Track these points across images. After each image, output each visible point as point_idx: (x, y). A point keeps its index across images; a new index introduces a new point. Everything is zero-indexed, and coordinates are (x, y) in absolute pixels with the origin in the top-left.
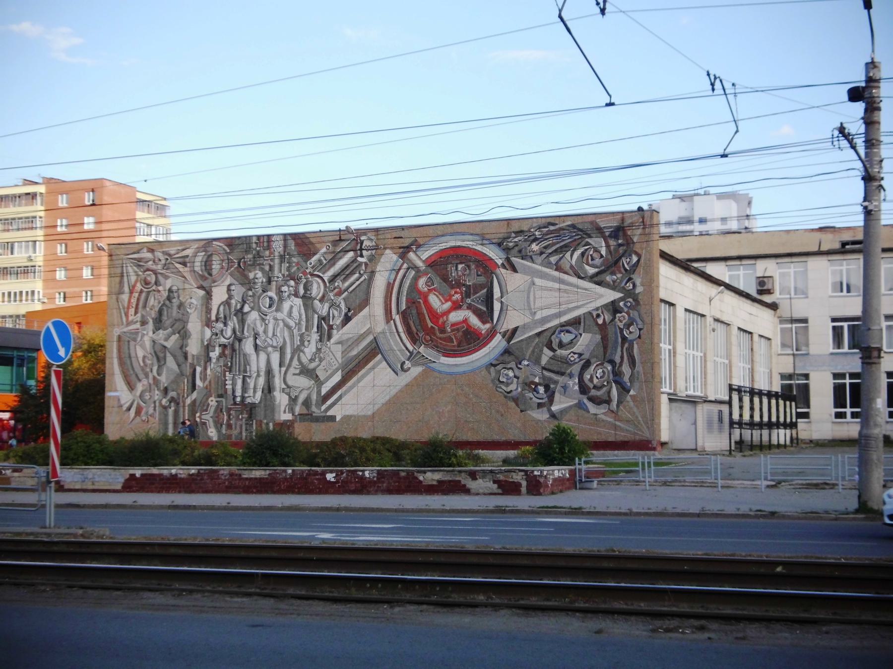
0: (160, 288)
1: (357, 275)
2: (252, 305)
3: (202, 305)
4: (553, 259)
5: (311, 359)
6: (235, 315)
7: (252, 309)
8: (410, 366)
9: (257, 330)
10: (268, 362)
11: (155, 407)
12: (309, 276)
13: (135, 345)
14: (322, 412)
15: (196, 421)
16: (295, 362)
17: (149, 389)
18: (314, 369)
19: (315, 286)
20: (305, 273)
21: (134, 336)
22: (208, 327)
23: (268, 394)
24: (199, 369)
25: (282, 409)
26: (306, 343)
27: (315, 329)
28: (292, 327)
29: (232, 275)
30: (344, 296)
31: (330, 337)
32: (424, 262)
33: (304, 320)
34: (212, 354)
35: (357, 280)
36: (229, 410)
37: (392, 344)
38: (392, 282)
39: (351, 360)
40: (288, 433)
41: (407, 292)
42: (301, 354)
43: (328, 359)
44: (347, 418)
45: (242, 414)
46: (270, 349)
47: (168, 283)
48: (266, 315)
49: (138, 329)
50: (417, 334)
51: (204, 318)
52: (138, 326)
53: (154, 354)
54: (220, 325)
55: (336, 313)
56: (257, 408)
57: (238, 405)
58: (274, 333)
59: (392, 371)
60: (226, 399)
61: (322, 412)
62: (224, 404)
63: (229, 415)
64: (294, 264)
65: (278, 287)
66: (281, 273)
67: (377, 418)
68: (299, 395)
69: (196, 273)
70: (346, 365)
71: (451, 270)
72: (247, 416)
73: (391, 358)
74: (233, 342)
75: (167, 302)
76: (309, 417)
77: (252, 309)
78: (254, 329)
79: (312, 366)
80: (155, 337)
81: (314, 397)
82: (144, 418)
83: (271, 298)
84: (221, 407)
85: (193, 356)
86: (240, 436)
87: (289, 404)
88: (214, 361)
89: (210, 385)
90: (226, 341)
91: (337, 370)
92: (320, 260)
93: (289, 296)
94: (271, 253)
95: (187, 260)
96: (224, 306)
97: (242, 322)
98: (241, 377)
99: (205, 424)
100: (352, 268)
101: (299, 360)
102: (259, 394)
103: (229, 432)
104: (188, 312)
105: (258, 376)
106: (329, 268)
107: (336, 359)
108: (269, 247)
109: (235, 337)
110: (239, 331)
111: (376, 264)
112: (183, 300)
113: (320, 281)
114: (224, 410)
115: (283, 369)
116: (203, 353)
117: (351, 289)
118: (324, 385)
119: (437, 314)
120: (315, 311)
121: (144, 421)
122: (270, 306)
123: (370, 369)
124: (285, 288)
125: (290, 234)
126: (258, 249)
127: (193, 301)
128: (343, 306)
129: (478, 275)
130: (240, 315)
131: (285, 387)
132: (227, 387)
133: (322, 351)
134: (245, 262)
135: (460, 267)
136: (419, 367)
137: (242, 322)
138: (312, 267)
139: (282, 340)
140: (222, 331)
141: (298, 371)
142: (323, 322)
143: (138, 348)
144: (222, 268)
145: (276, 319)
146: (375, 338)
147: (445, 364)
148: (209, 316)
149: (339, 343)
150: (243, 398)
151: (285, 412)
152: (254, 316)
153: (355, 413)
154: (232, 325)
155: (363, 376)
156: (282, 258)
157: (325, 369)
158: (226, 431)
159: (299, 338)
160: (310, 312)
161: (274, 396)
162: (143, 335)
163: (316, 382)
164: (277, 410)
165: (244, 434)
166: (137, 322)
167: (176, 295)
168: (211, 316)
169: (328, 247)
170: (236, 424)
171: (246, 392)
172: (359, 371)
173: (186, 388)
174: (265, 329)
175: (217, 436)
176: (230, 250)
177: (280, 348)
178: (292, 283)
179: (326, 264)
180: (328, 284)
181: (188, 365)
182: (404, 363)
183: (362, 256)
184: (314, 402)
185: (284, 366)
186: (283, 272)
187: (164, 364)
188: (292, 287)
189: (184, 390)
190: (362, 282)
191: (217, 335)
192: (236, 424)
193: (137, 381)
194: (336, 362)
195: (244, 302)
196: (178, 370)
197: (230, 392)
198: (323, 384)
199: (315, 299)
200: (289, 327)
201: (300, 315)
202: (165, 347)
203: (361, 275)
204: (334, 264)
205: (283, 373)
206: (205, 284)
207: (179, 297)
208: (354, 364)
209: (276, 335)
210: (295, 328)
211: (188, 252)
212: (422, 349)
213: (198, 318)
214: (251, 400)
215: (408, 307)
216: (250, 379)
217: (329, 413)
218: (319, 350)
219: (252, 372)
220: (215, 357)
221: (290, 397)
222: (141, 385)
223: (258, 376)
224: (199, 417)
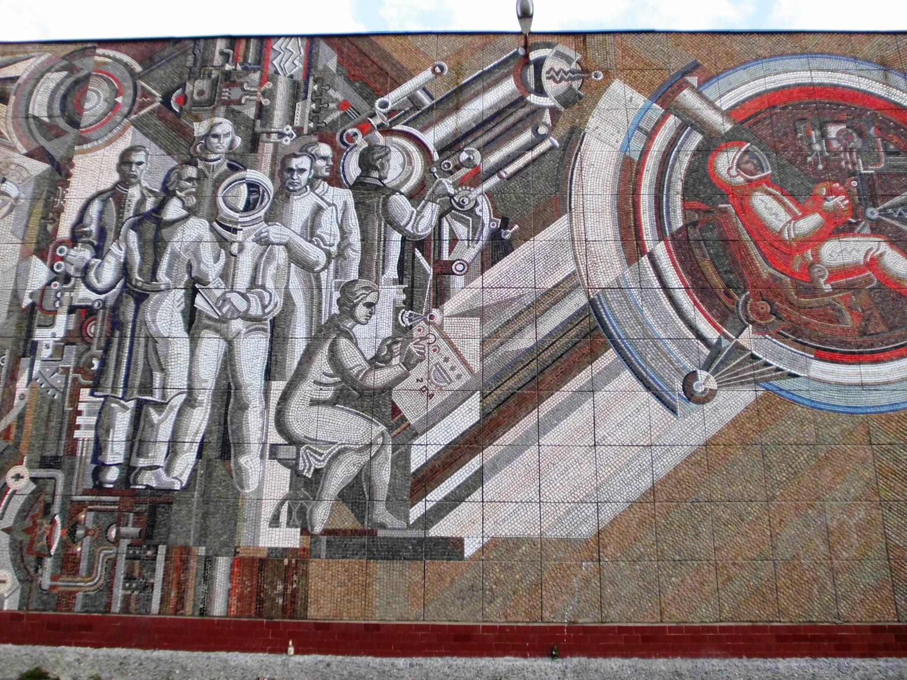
1: (526, 136)
2: (193, 201)
3: (34, 199)
5: (376, 357)
6: (134, 227)
8: (713, 384)
9: (199, 271)
10: (228, 362)
12: (377, 134)
14: (410, 527)
16: (321, 364)
18: (387, 389)
19: (395, 161)
20: (365, 128)
22: (43, 259)
23: (219, 464)
25: (267, 512)
27: (392, 272)
28: (317, 263)
29: (140, 125)
30: (487, 185)
31: (441, 295)
32: (728, 114)
33: (358, 246)
34: (42, 335)
35: (530, 147)
36: (72, 511)
37: (651, 320)
38: (637, 159)
39: (515, 362)
40: (283, 595)
41: (685, 183)
42: (343, 342)
43: (436, 358)
45: (119, 523)
46: (237, 325)
48: (235, 231)
50: (728, 295)
54: (84, 254)
55: (462, 231)
56: (175, 507)
57: (109, 492)
58: (254, 279)
59: (653, 400)
60: (70, 473)
61: (410, 527)
62: (60, 489)
64: (332, 106)
65: (279, 158)
66: (292, 124)
67: (610, 549)
68: (329, 467)
69: (31, 120)
70: (497, 377)
71: (810, 137)
72: (136, 530)
73: (653, 365)
74: (119, 300)
76: (365, 540)
77: (192, 212)
78: (190, 266)
79: (381, 377)
81: (384, 475)
83: (253, 187)
84: (48, 499)
86: (105, 600)
87: (291, 498)
88: (45, 353)
89: (20, 427)
90: (94, 296)
91: (465, 393)
92: (412, 98)
93: (311, 183)
94: (263, 80)
95: (12, 87)
96: (105, 202)
97: (156, 247)
98: (131, 404)
100: (511, 120)
101: (334, 357)
102: (186, 461)
103: (63, 583)
105: (190, 402)
106: (442, 118)
107: (465, 363)
108: (262, 60)
109: (125, 286)
110: (140, 271)
111: (584, 116)
113: (411, 147)
114: (56, 509)
115: (278, 386)
116: (12, 330)
117: (510, 169)
118: (421, 439)
119: (783, 241)
120: (392, 223)
122: (250, 206)
123: (581, 391)
125: (328, 38)
126: (228, 67)
128: (485, 211)
129: (889, 153)
130: (150, 228)
131: (280, 440)
132: (77, 434)
133: (416, 334)
134: (183, 99)
135: (833, 131)
136: (745, 388)
138: (389, 114)
139: (279, 300)
140: (87, 268)
141: (328, 394)
142: (418, 254)
144: (114, 107)
145: (264, 242)
146: (592, 302)
147: (829, 383)
148: (50, 228)
149: (480, 313)
150: (129, 470)
151: (275, 521)
153: (535, 533)
154: (122, 254)
155: (560, 414)
156: (297, 92)
157: (423, 390)
158: (54, 578)
159: (337, 295)
160: (377, 225)
161: (239, 468)
163: (390, 428)
164: (248, 513)
165: (119, 592)
168: (56, 230)
169: (438, 70)
170: (92, 557)
171: (139, 455)
172: (541, 400)
174: (227, 265)
175: (17, 595)
176: (145, 69)
177: (273, 322)
178: (325, 149)
179: (431, 108)
180: (436, 157)
182: (692, 376)
183: (540, 91)
184: (382, 493)
185: (282, 378)
186: (297, 123)
188: (324, 158)
190: (543, 154)
191: (67, 278)
192: (92, 557)
194: (461, 369)
195: (167, 193)
197: (85, 451)
198: (416, 435)
199: (394, 191)
200: (306, 266)
201: (344, 234)
203: (542, 138)
204: (457, 108)
206: (56, 148)
208: (524, 375)
209: (263, 287)
210: (326, 267)
211: (21, 70)
212: (747, 338)
213: (13, 232)
214: (158, 477)
215: (689, 224)
216: (160, 412)
217: (438, 530)
218: (402, 332)
219: (170, 393)
220: (51, 342)
221: (296, 474)
223: (190, 402)
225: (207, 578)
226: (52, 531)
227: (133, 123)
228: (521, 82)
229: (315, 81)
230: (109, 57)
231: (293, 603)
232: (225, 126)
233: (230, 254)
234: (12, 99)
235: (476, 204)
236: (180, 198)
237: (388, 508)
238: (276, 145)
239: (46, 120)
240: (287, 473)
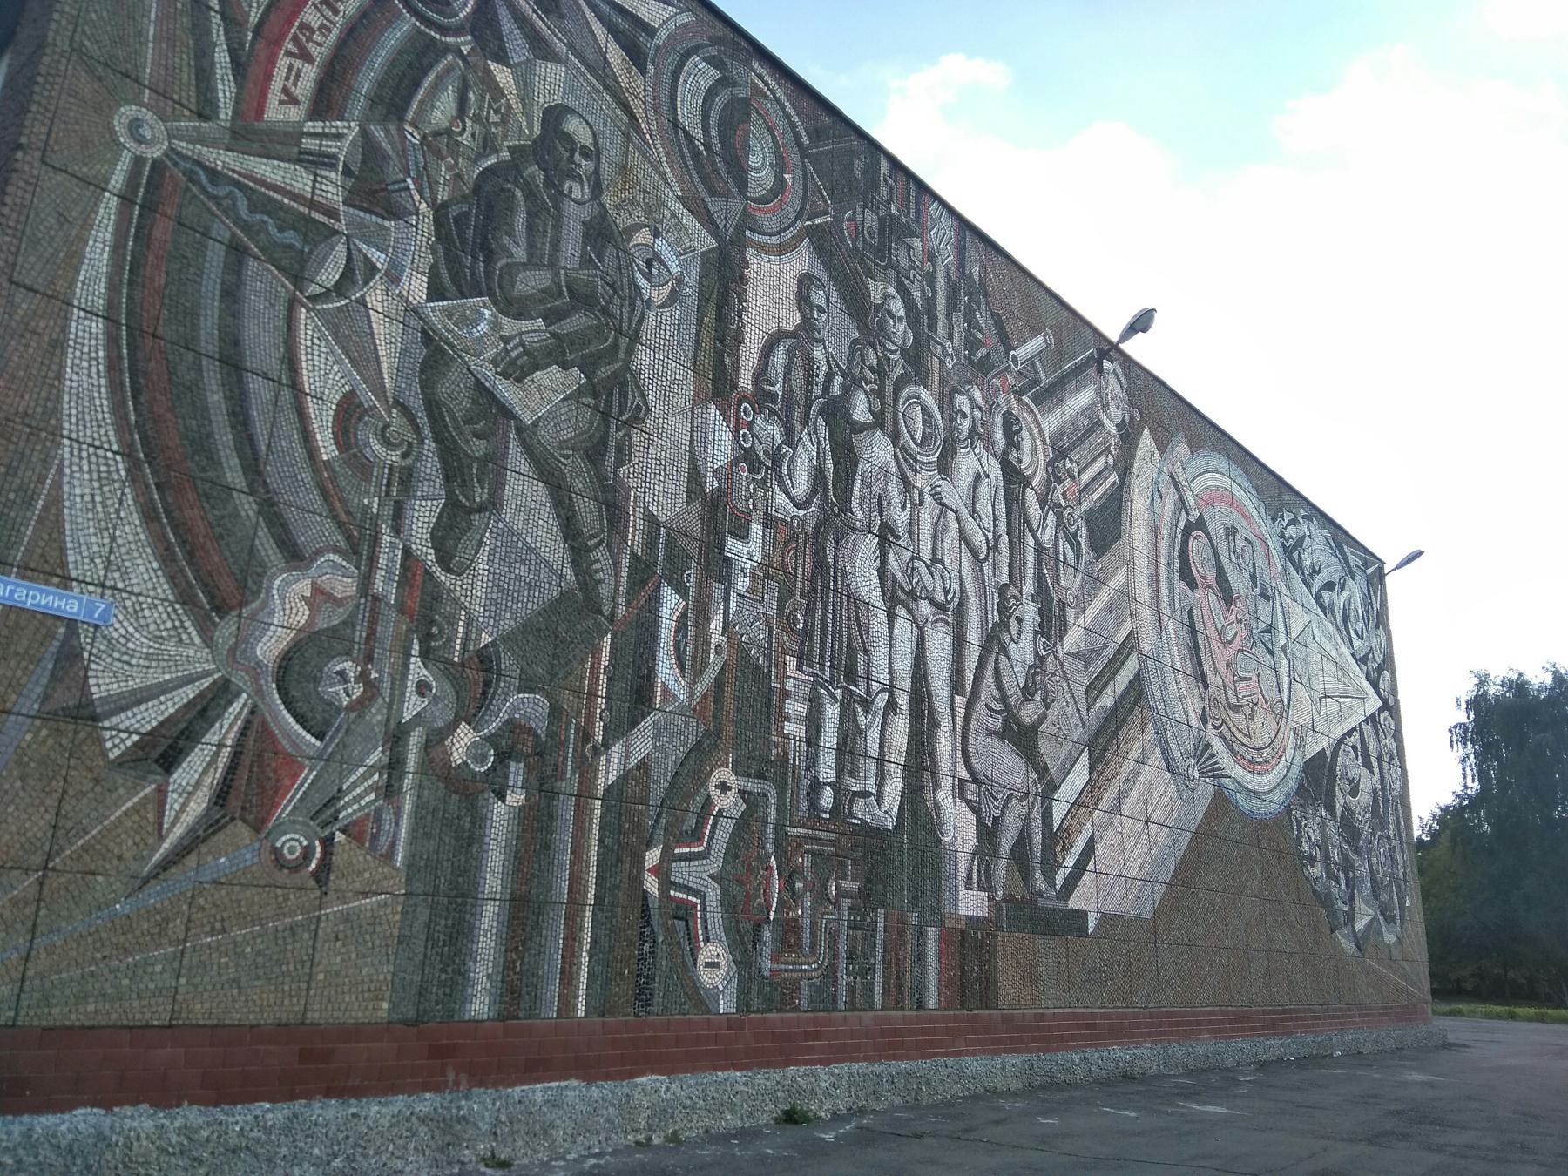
0: (503, 76)
1: (1099, 464)
4: (1326, 595)
6: (821, 412)
7: (879, 421)
11: (394, 766)
13: (292, 305)
15: (645, 895)
17: (360, 634)
18: (1035, 727)
21: (290, 237)
24: (671, 602)
26: (1013, 624)
27: (1029, 587)
42: (1002, 658)
44: (1106, 919)
46: (925, 609)
47: (551, 82)
48: (916, 471)
49: (332, 213)
51: (707, 360)
52: (332, 190)
53: (422, 419)
63: (789, 877)
68: (1003, 814)
69: (680, 132)
75: (534, 171)
80: (435, 311)
82: (291, 843)
85: (651, 519)
88: (743, 583)
90: (790, 506)
93: (973, 433)
99: (684, 913)
102: (894, 787)
104: (638, 289)
105: (892, 705)
107: (1079, 711)
112: (623, 221)
115: (960, 701)
116: (696, 529)
121: (296, 867)
124: (961, 401)
127: (661, 246)
131: (967, 776)
137: (846, 457)
139: (956, 586)
140: (776, 458)
141: (996, 723)
143: (307, 326)
148: (727, 361)
152: (878, 451)
157: (1056, 736)
158: (775, 958)
159: (997, 599)
162: (355, 273)
165: (844, 980)
166: (329, 161)
167: (586, 166)
171: (852, 774)
173: (603, 689)
181: (626, 562)
187: (481, 509)
188: (980, 409)
189: (593, 695)
193: (268, 549)
196: (570, 577)
202: (507, 413)
205: (960, 712)
207: (597, 189)
210: (986, 559)
219: (875, 686)
222: (303, 587)
224: (655, 871)
225: (921, 957)
226: (768, 879)
227: (811, 232)
228: (1098, 392)
229: (965, 295)
230: (767, 84)
231: (987, 988)
232: (897, 306)
233: (913, 506)
234: (651, 70)
235: (1078, 529)
236: (866, 392)
237: (1043, 873)
238: (942, 363)
239: (701, 148)
240: (972, 818)
